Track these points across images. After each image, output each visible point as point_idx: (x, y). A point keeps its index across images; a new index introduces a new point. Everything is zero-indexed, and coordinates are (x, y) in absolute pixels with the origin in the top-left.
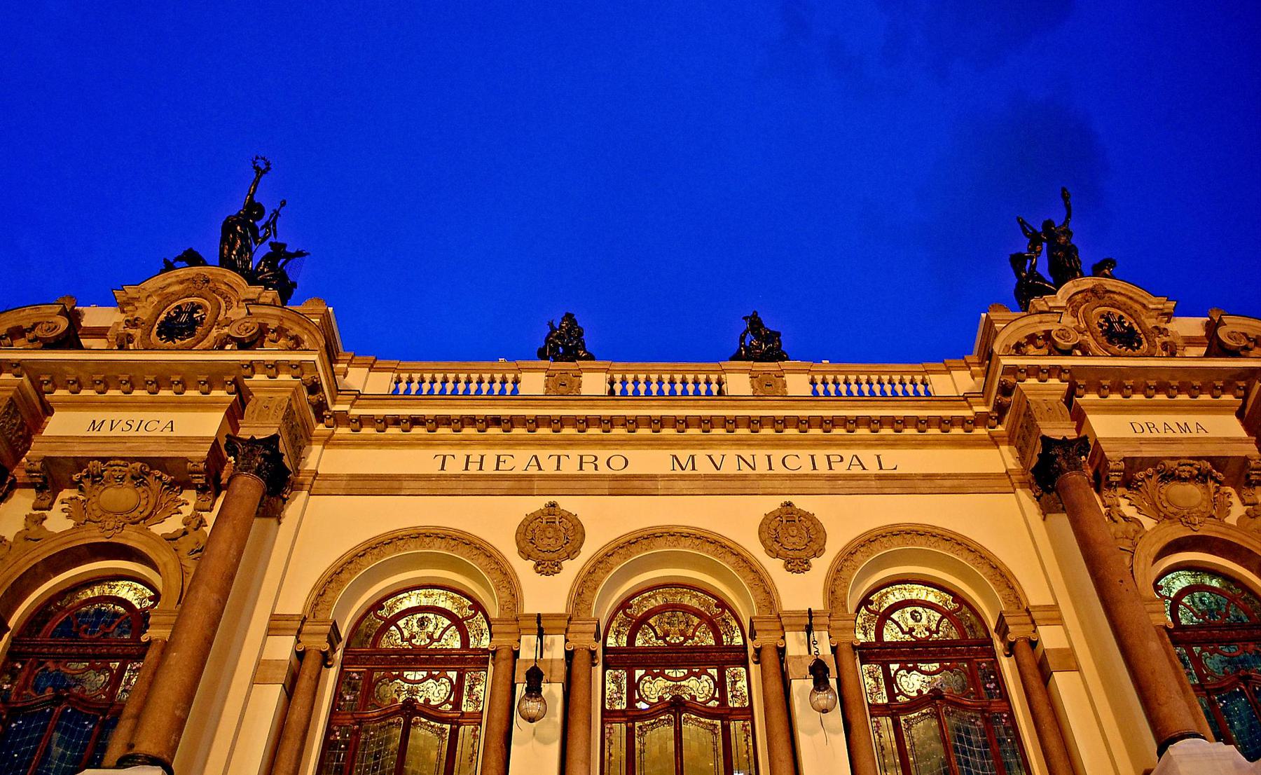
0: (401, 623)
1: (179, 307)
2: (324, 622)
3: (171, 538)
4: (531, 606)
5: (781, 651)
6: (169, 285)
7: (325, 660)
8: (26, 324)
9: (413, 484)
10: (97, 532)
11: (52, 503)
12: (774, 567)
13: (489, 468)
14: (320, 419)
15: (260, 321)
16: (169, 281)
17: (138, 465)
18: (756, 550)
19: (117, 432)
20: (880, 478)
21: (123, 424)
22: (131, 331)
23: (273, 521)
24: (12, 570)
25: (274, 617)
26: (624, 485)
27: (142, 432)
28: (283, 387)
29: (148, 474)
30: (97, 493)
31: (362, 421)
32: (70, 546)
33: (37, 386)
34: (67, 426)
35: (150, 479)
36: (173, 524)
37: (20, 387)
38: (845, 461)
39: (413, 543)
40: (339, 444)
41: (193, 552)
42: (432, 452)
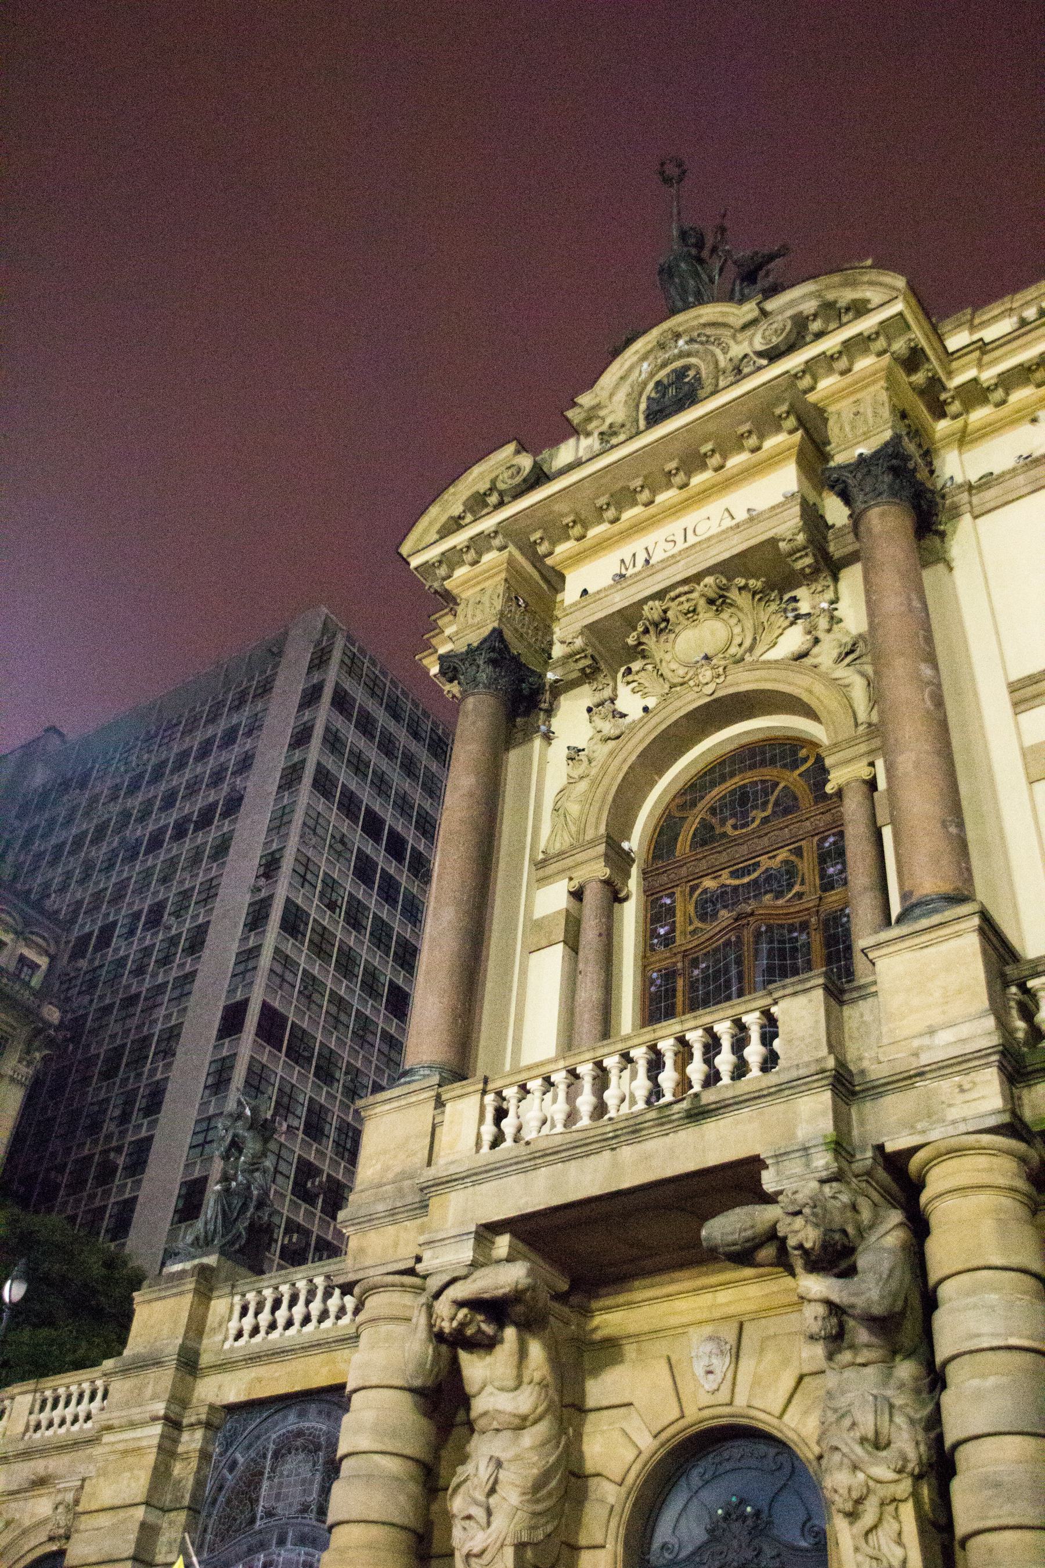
1: (658, 383)
8: (483, 486)
14: (939, 411)
17: (709, 580)
21: (663, 545)
23: (941, 567)
24: (605, 782)
25: (1014, 688)
27: (692, 539)
28: (866, 381)
30: (669, 646)
32: (664, 726)
33: (530, 550)
34: (593, 580)
35: (733, 595)
40: (984, 436)
41: (840, 659)
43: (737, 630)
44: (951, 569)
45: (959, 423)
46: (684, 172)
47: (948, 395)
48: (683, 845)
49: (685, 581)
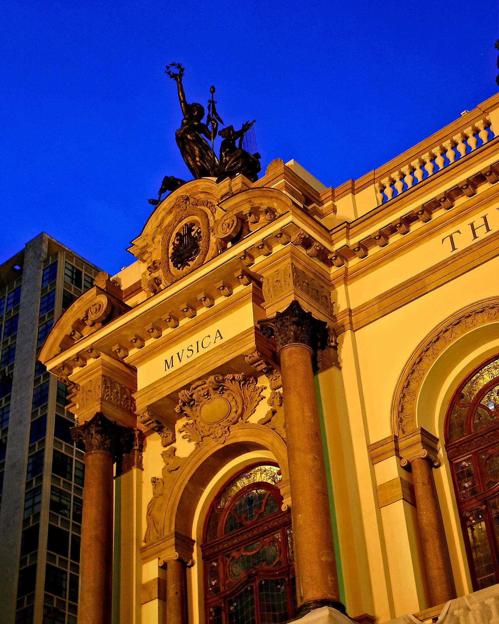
0: (484, 401)
1: (178, 234)
2: (413, 433)
3: (266, 422)
6: (163, 220)
7: (431, 463)
8: (81, 316)
9: (433, 277)
10: (213, 443)
11: (174, 436)
14: (330, 263)
15: (235, 212)
16: (160, 217)
17: (212, 378)
19: (185, 361)
21: (186, 351)
22: (155, 275)
23: (334, 369)
24: (172, 498)
27: (202, 351)
29: (224, 381)
30: (198, 413)
31: (363, 247)
32: (201, 462)
34: (152, 375)
35: (227, 384)
36: (263, 410)
37: (103, 364)
39: (457, 329)
40: (358, 275)
42: (438, 239)
43: (233, 404)
44: (340, 368)
45: (342, 269)
46: (182, 70)
47: (333, 255)
48: (221, 525)
49: (199, 379)
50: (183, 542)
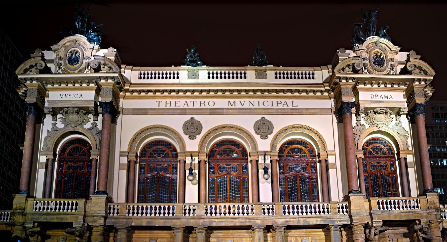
2: (134, 153)
3: (90, 129)
4: (188, 149)
5: (257, 161)
9: (151, 111)
12: (257, 137)
13: (173, 106)
17: (76, 109)
18: (252, 132)
19: (67, 99)
20: (292, 109)
21: (68, 96)
22: (60, 62)
26: (214, 111)
35: (80, 112)
36: (88, 126)
37: (39, 85)
38: (282, 103)
39: (154, 130)
50: (55, 155)
